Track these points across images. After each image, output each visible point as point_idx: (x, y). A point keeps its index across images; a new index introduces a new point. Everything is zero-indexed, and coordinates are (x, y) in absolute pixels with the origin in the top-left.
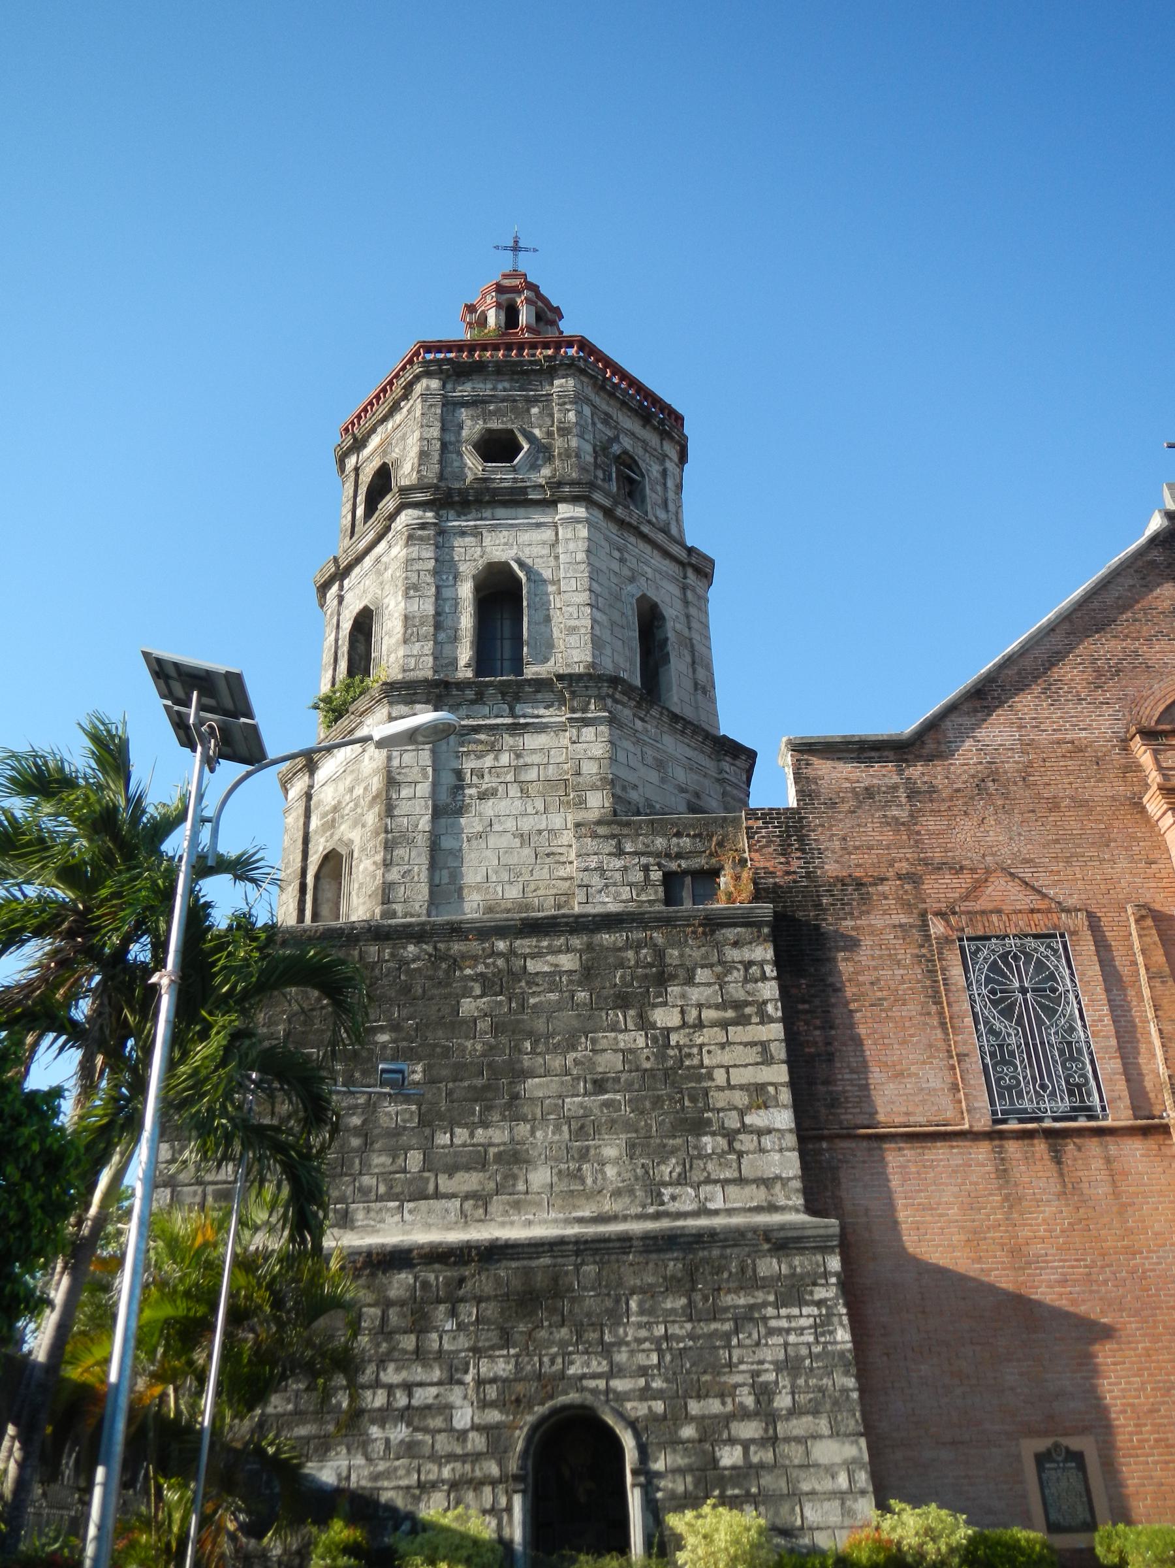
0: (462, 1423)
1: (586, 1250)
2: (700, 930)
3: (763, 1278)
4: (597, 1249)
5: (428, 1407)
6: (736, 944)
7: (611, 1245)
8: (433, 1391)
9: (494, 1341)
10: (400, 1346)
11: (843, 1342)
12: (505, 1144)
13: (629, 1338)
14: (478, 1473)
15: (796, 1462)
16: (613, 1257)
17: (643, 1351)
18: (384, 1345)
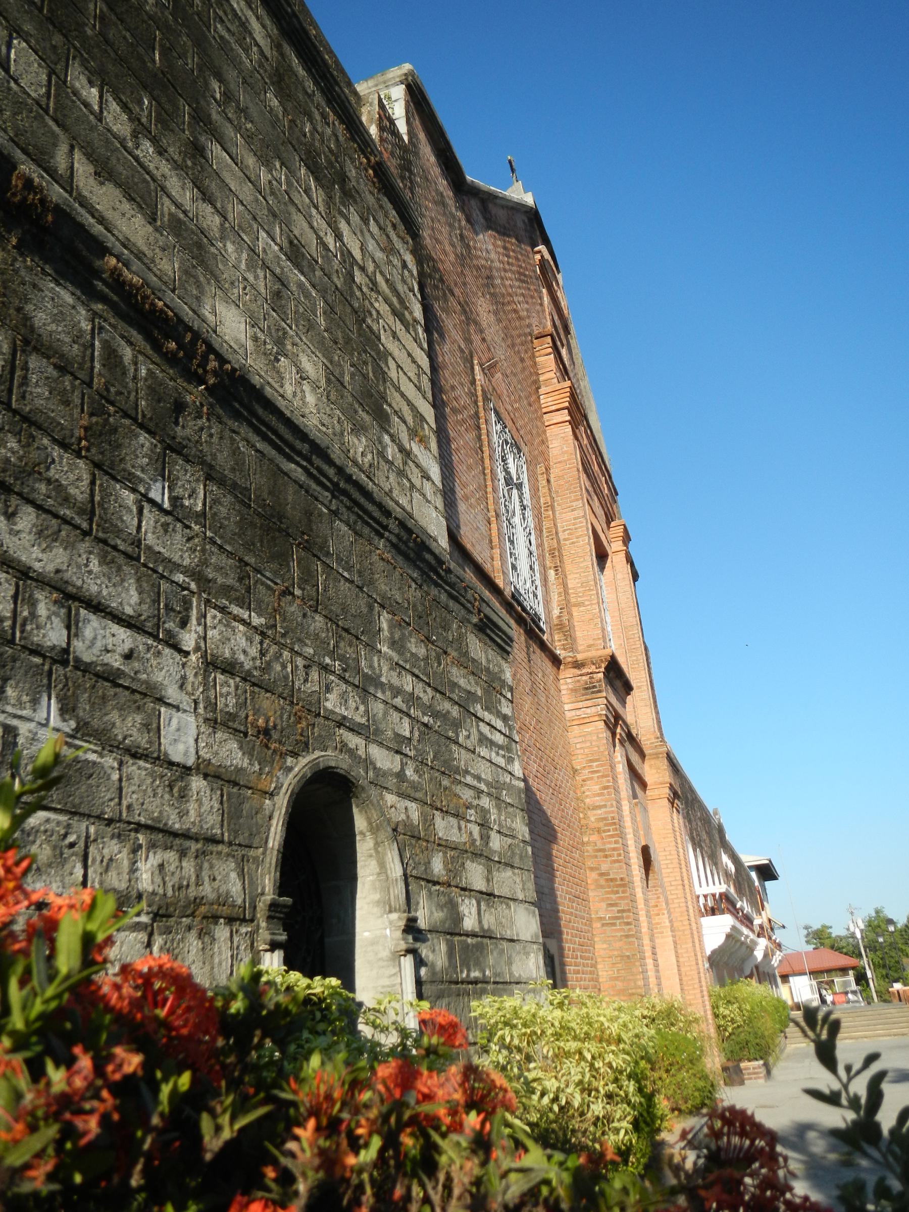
0: (181, 747)
1: (345, 493)
2: (371, 172)
3: (474, 660)
4: (356, 503)
5: (111, 677)
6: (394, 226)
7: (370, 507)
8: (123, 638)
9: (231, 581)
10: (52, 473)
11: (519, 778)
12: (185, 212)
13: (383, 679)
14: (207, 890)
15: (508, 934)
16: (366, 531)
17: (396, 708)
18: (12, 444)
